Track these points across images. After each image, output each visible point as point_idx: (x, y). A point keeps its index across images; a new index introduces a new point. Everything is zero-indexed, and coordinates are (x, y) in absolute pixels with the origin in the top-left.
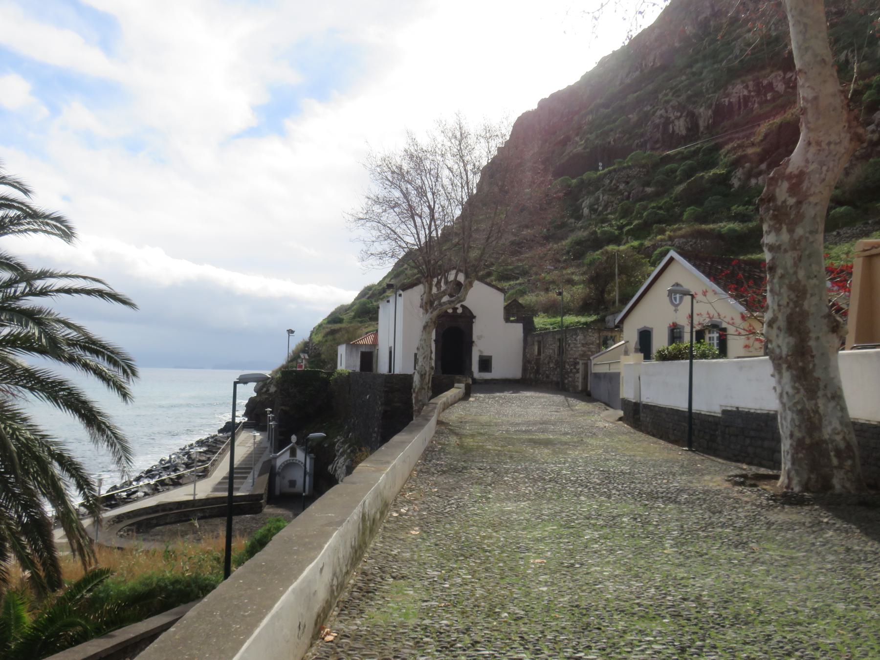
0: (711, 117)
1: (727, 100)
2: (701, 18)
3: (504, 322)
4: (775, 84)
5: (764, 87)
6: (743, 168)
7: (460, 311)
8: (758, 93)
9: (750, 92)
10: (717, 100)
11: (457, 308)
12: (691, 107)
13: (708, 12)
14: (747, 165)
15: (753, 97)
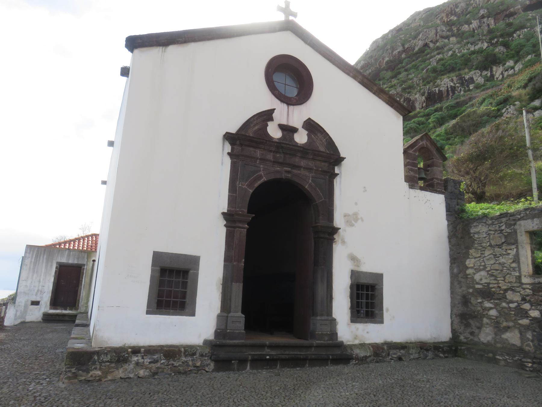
0: (425, 102)
1: (437, 89)
2: (396, 52)
3: (406, 185)
4: (475, 79)
5: (466, 81)
6: (514, 105)
7: (301, 138)
8: (462, 84)
9: (454, 84)
10: (429, 90)
11: (294, 130)
12: (407, 95)
13: (400, 49)
14: (517, 103)
15: (458, 87)
